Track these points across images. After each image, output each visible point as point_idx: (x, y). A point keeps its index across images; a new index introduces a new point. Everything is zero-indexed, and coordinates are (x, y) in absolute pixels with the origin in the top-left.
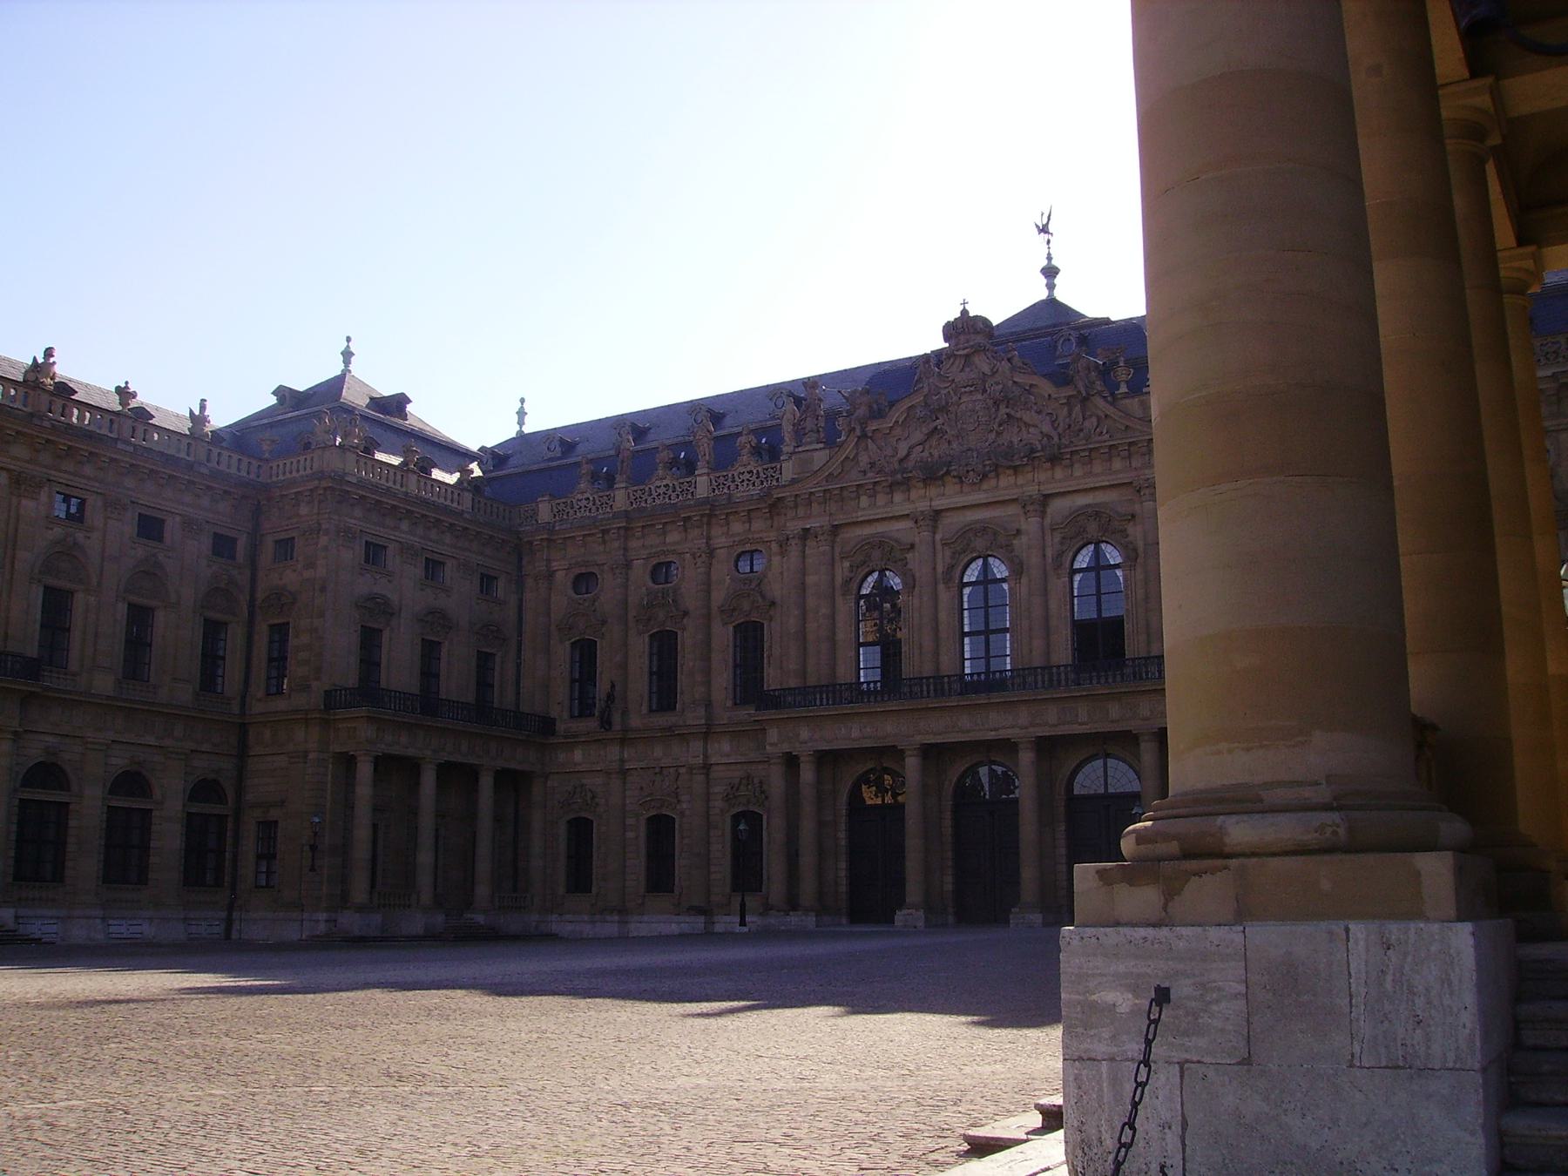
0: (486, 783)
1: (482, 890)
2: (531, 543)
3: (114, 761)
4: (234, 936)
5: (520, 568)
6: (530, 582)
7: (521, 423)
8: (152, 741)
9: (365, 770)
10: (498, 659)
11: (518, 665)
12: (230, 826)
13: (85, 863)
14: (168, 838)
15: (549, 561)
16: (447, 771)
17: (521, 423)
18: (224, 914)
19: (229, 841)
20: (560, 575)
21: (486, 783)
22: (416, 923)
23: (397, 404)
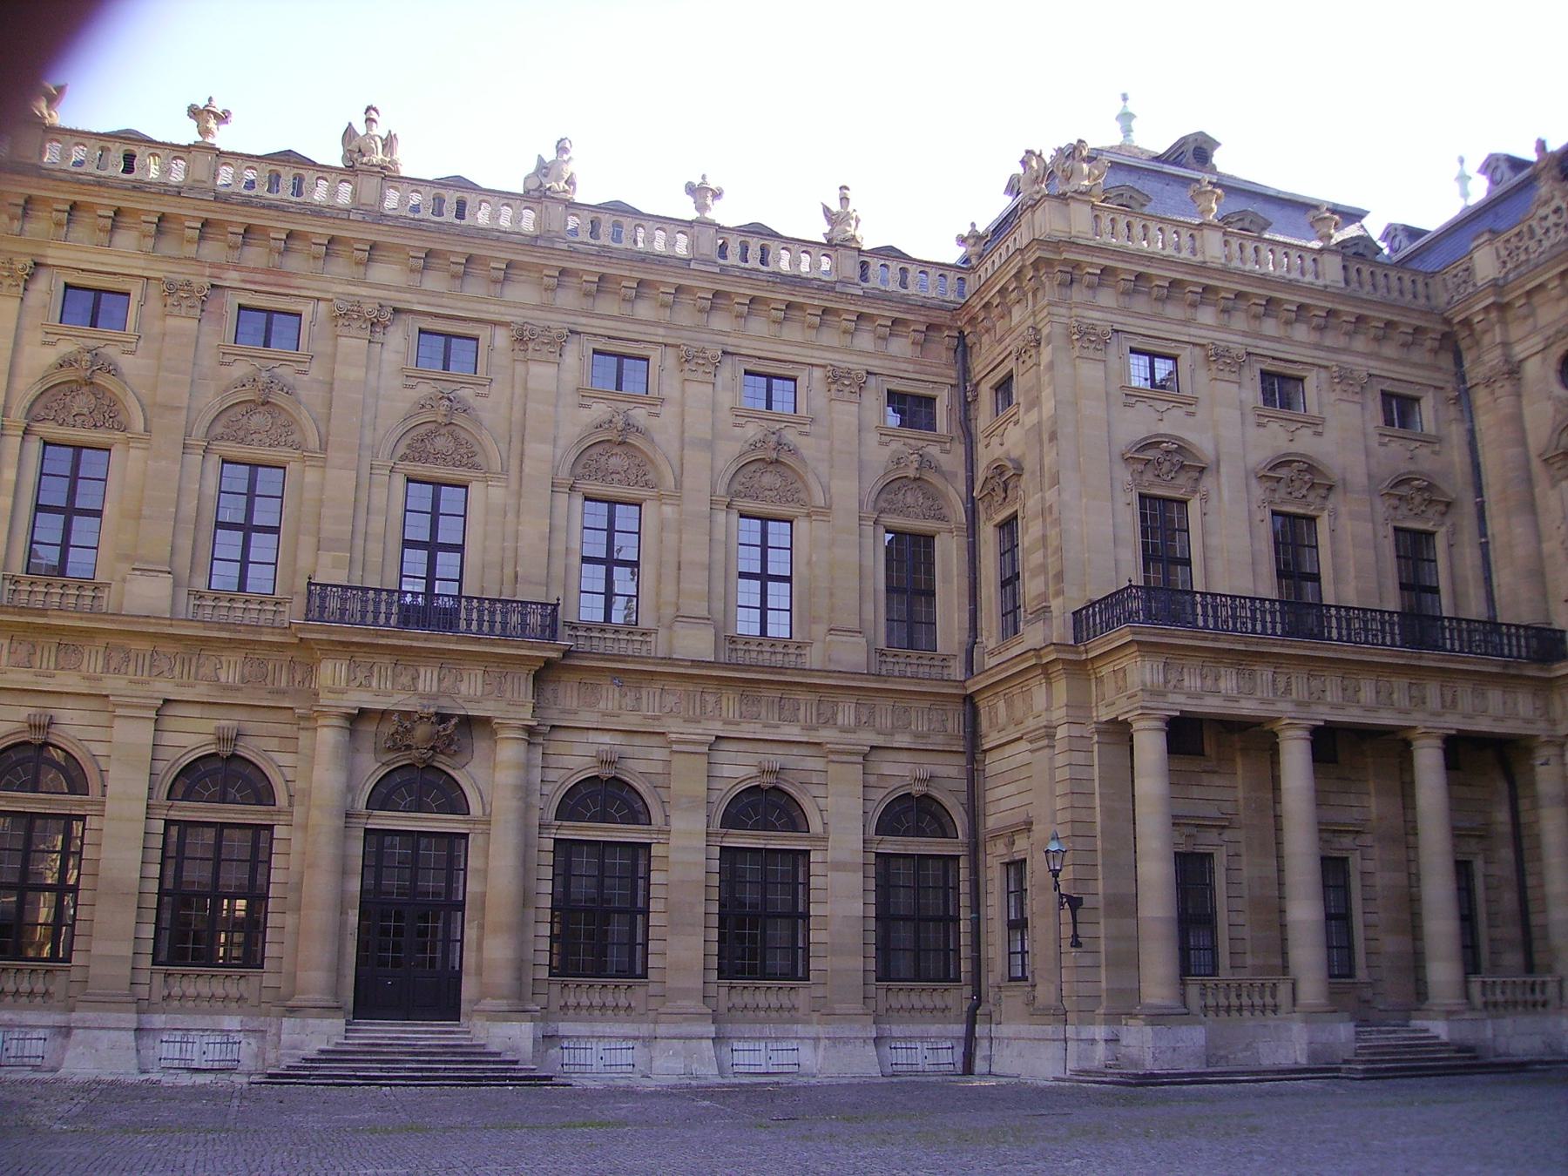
0: (1428, 761)
1: (1442, 972)
2: (1467, 323)
3: (727, 771)
4: (980, 1065)
5: (1462, 378)
6: (1481, 397)
7: (1465, 195)
8: (792, 732)
9: (1150, 746)
10: (1440, 543)
11: (1484, 548)
12: (964, 874)
13: (681, 938)
14: (840, 901)
15: (1506, 344)
16: (1332, 745)
17: (1465, 195)
18: (960, 1029)
19: (964, 900)
20: (1532, 369)
21: (1428, 761)
22: (1290, 1043)
23: (1198, 150)
